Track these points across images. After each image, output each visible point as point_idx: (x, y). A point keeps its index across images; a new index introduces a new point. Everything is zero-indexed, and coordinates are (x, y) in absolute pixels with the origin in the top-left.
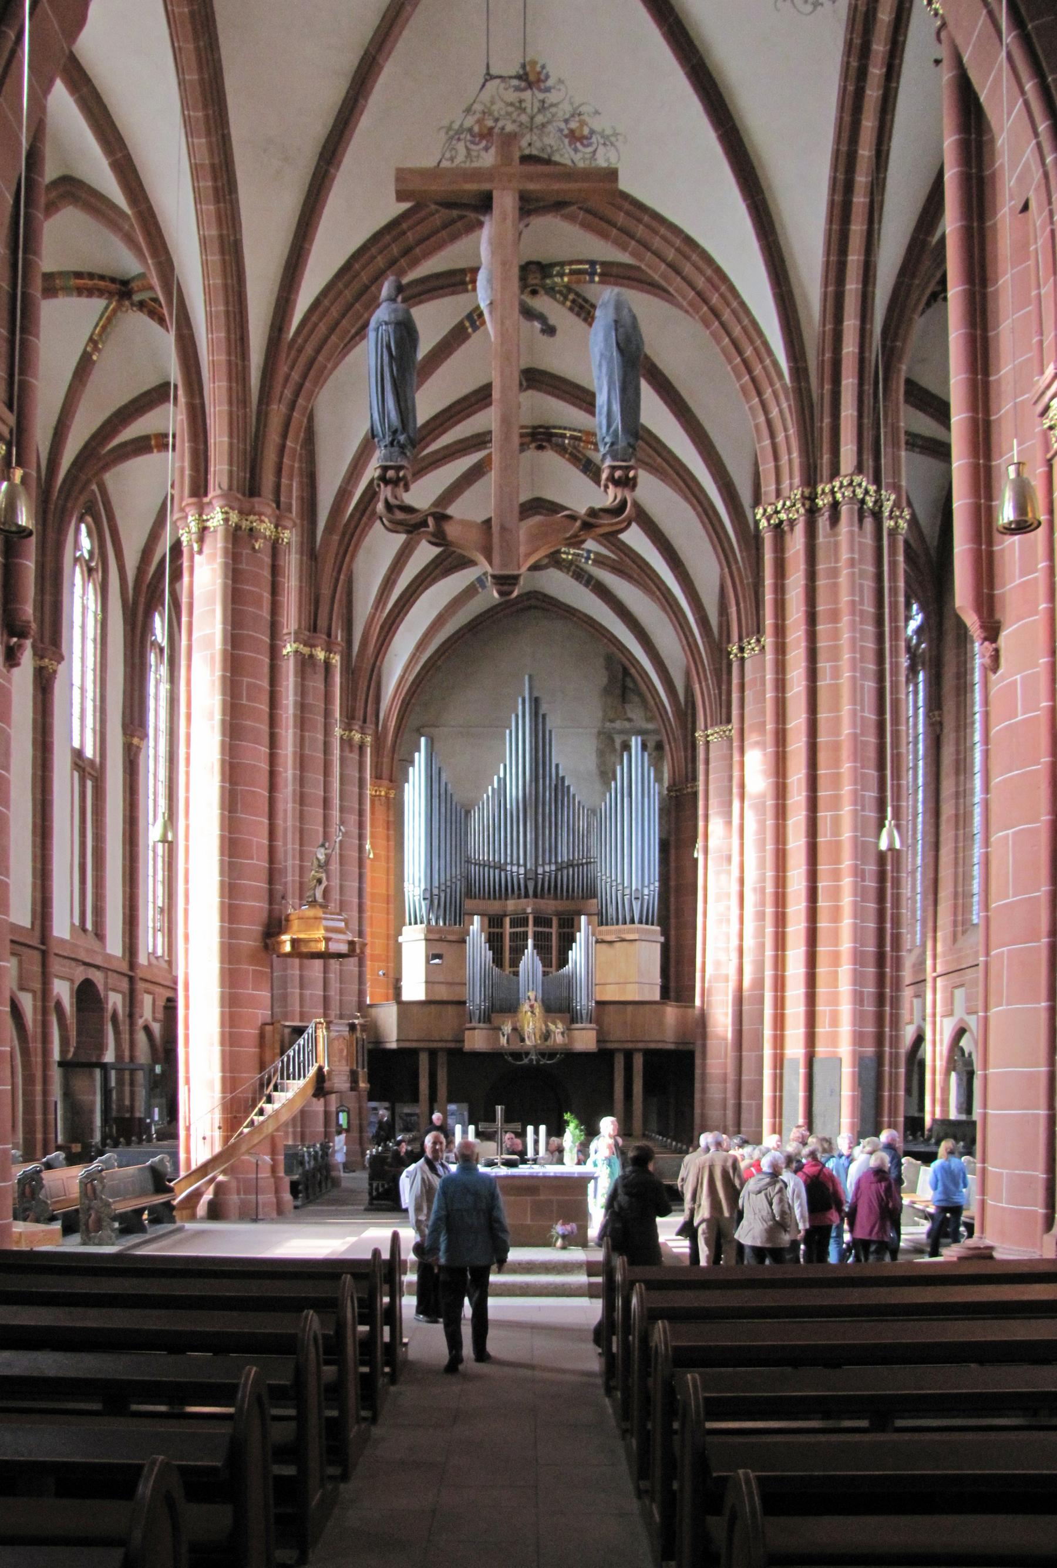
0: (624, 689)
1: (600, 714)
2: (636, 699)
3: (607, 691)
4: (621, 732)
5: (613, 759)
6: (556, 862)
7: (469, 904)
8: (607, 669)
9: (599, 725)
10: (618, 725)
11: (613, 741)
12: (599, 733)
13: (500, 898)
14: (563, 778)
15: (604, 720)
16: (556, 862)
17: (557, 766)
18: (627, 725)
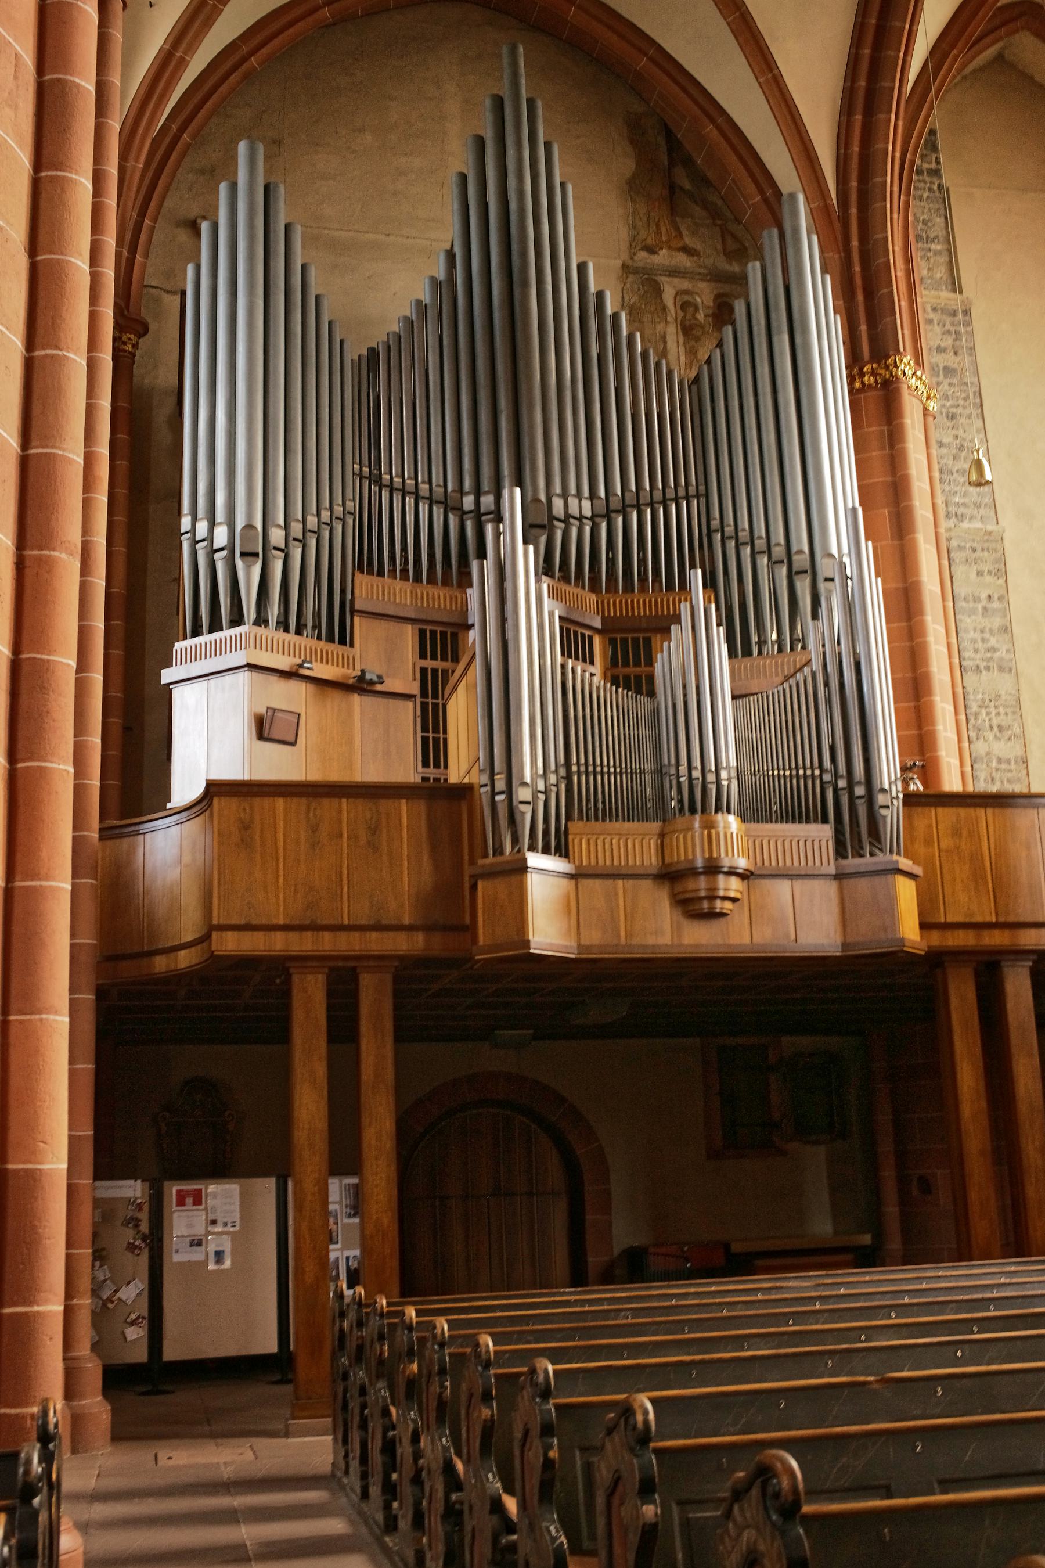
0: (673, 188)
1: (624, 233)
2: (698, 211)
3: (633, 187)
4: (674, 272)
5: (660, 327)
6: (593, 495)
7: (367, 590)
8: (632, 142)
9: (625, 256)
10: (663, 258)
11: (658, 292)
12: (624, 266)
13: (446, 582)
14: (600, 296)
15: (635, 244)
16: (593, 495)
17: (582, 268)
18: (682, 260)
